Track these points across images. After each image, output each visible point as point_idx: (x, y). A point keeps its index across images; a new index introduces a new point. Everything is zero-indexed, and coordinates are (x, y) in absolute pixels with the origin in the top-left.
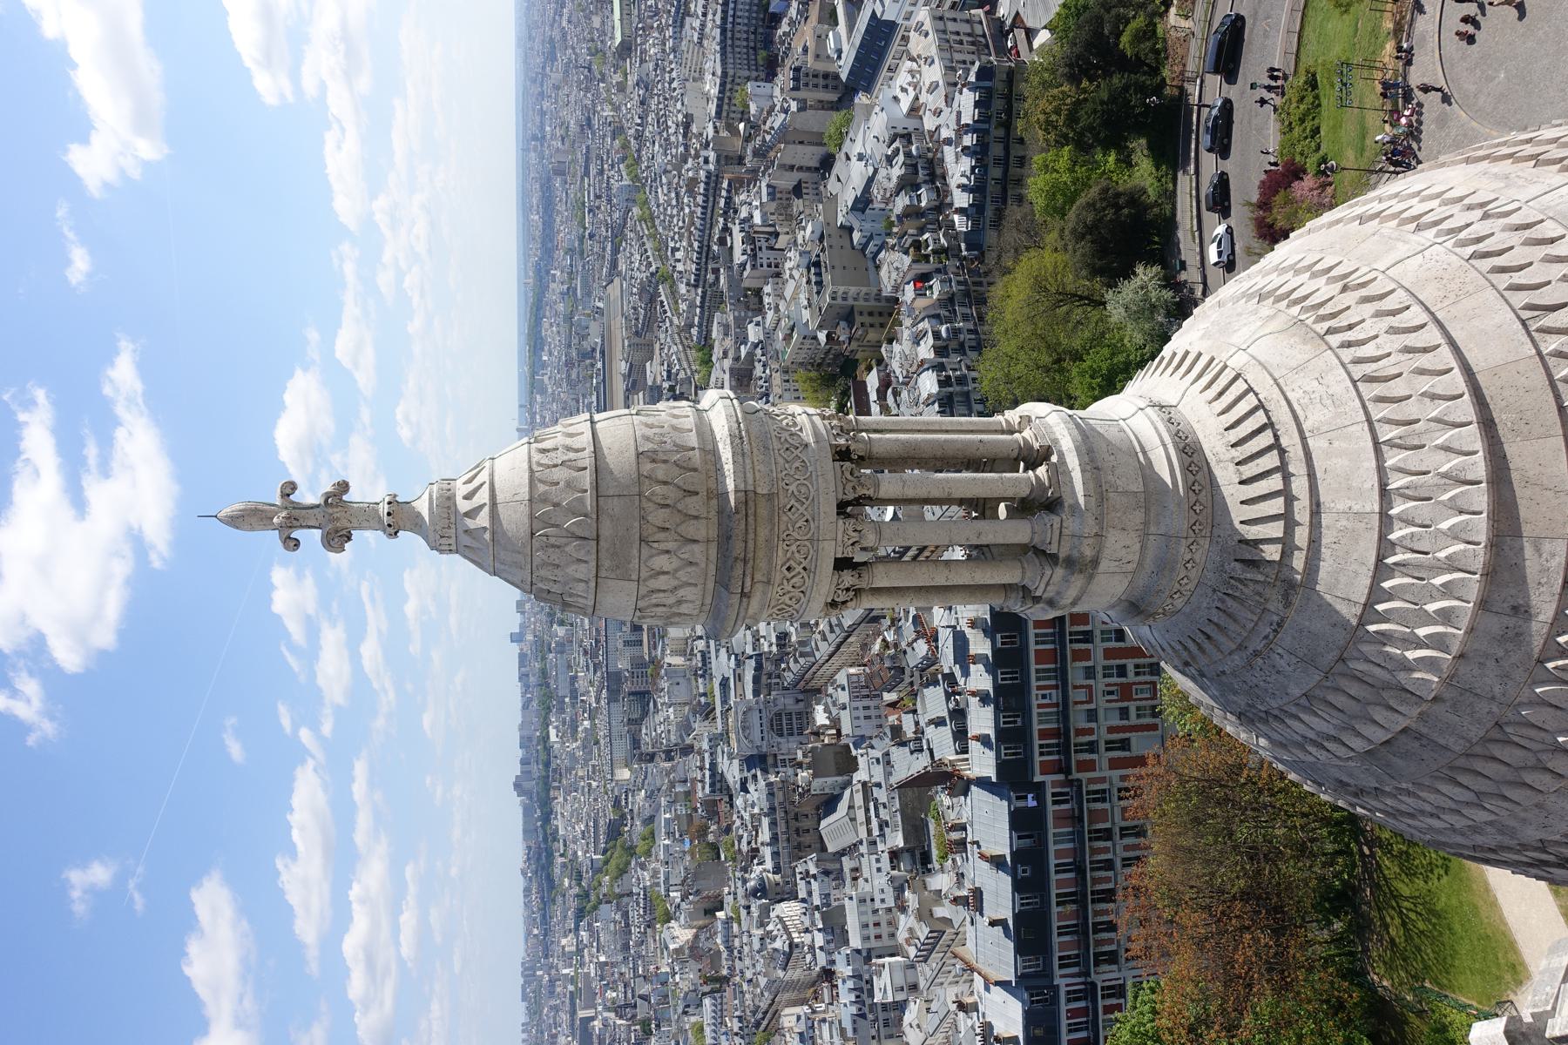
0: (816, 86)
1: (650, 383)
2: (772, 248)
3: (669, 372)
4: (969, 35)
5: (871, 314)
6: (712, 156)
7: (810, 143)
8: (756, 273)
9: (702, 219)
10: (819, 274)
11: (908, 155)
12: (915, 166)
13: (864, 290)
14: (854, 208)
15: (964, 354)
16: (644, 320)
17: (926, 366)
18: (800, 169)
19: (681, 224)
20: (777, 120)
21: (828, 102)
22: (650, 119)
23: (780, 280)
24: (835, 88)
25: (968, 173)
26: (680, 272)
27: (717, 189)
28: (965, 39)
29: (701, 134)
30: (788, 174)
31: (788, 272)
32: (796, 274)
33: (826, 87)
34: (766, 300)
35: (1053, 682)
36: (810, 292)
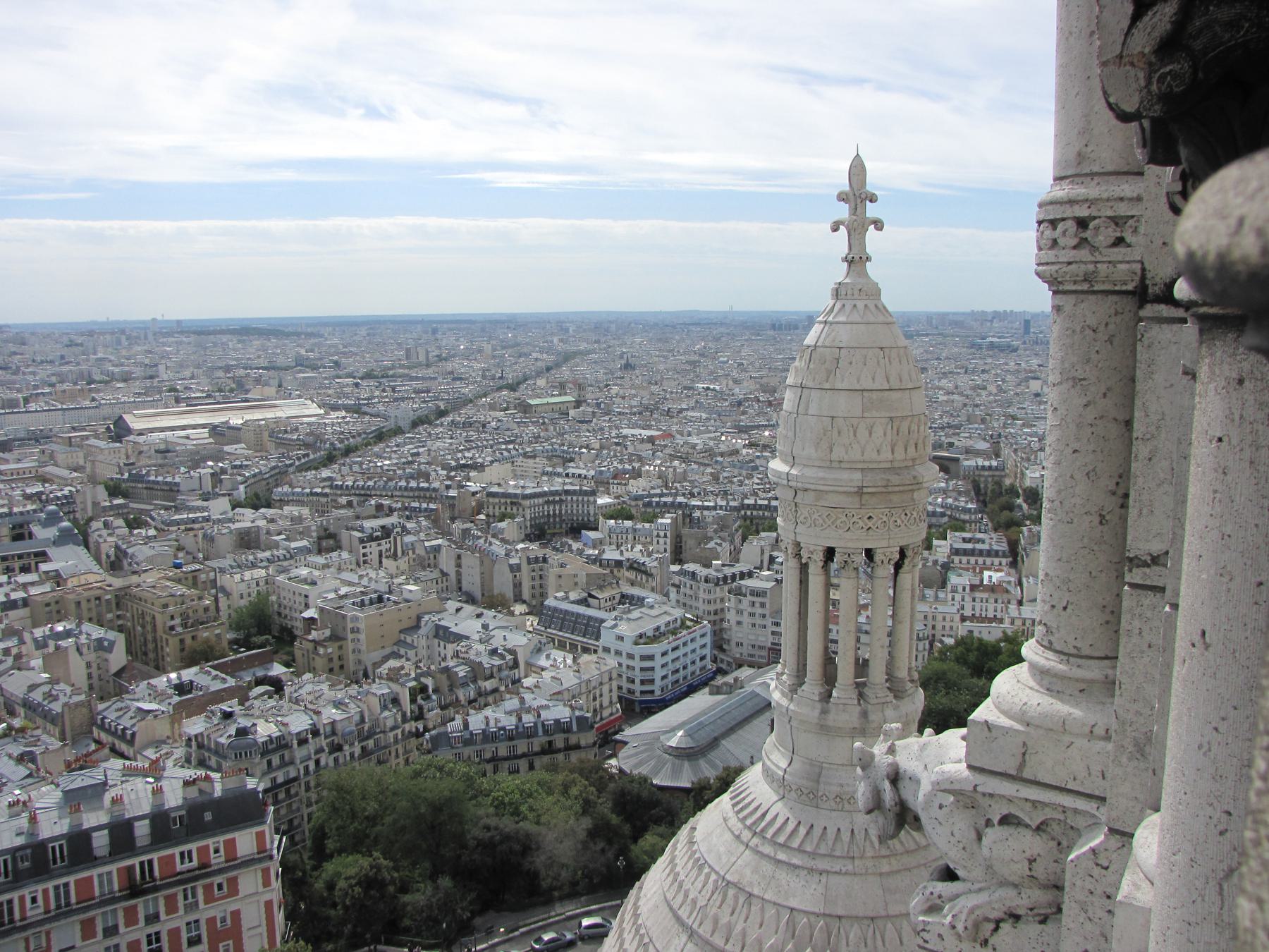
0: (533, 579)
1: (227, 448)
2: (380, 556)
3: (241, 467)
4: (601, 705)
5: (340, 658)
6: (452, 493)
7: (482, 578)
8: (356, 543)
9: (395, 488)
10: (371, 603)
11: (500, 668)
12: (492, 676)
13: (363, 648)
14: (438, 627)
15: (330, 753)
16: (285, 439)
17: (315, 717)
18: (459, 574)
19: (385, 468)
20: (497, 548)
21: (521, 592)
22: (472, 433)
23: (353, 567)
24: (533, 596)
25: (500, 725)
26: (340, 470)
27: (431, 500)
28: (598, 703)
29: (469, 480)
30: (453, 563)
31: (365, 573)
32: (365, 581)
33: (533, 587)
34: (335, 554)
35: (53, 905)
36: (354, 595)
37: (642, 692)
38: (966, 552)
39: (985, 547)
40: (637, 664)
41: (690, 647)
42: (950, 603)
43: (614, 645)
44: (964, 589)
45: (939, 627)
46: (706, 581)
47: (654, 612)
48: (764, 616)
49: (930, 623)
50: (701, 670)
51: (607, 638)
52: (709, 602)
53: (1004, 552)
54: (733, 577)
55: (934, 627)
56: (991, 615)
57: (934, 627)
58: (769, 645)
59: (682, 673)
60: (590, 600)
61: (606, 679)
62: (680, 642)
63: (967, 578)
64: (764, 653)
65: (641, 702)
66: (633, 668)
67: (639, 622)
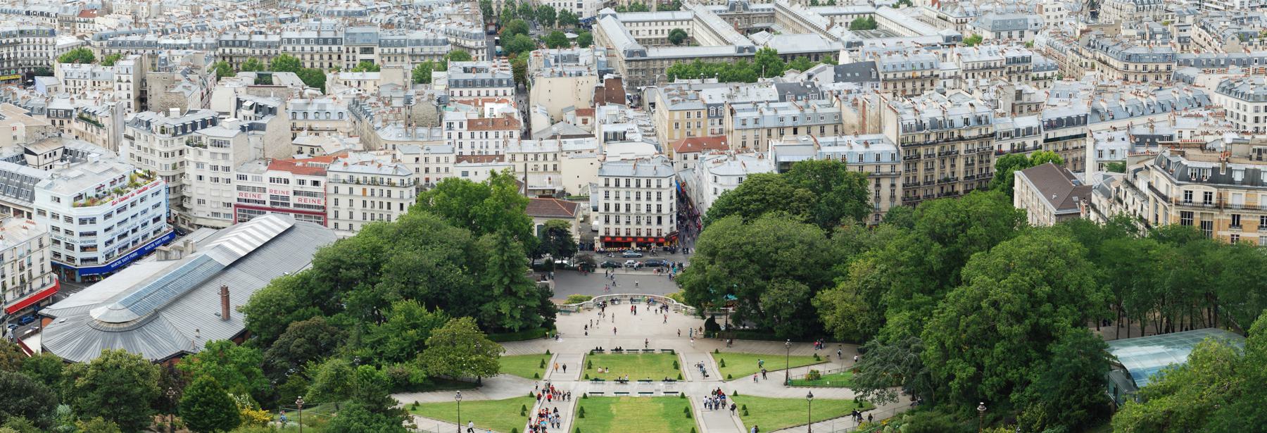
37: (82, 260)
38: (466, 84)
39: (487, 76)
40: (76, 228)
41: (140, 207)
42: (446, 143)
43: (50, 207)
44: (461, 126)
45: (433, 169)
46: (163, 132)
47: (98, 170)
48: (227, 169)
49: (422, 167)
50: (155, 233)
51: (42, 200)
52: (166, 155)
53: (508, 81)
54: (194, 126)
55: (427, 170)
56: (492, 152)
57: (427, 170)
58: (236, 202)
59: (131, 237)
60: (27, 156)
61: (35, 245)
62: (128, 202)
63: (463, 113)
64: (231, 211)
65: (82, 271)
66: (58, 230)
67: (81, 181)
